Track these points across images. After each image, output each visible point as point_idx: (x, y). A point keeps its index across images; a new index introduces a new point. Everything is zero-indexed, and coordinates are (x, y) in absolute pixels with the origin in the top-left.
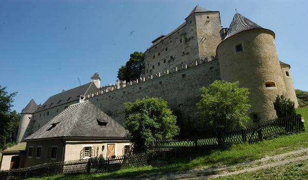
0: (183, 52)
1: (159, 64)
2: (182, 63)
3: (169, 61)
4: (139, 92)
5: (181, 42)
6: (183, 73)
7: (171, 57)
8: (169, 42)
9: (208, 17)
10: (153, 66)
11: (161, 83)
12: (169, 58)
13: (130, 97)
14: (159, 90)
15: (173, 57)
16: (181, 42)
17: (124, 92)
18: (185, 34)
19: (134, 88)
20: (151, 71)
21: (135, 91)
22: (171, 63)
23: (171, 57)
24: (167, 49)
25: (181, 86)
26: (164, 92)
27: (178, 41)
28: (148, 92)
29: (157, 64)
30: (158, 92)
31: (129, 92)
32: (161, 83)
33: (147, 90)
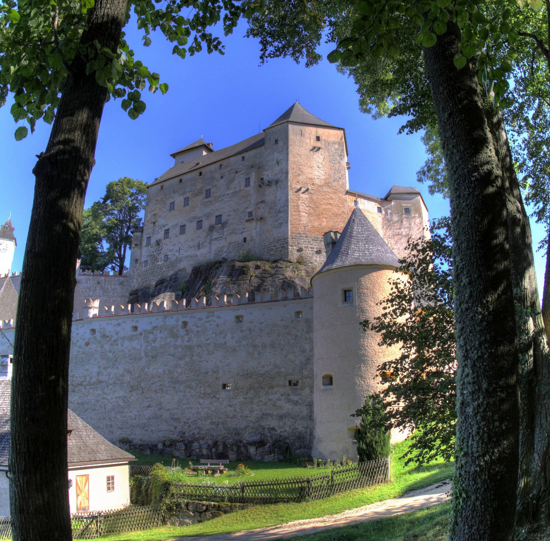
0: (250, 214)
1: (183, 229)
2: (245, 239)
3: (212, 228)
4: (131, 338)
5: (247, 184)
6: (239, 313)
8: (218, 176)
9: (318, 139)
10: (167, 232)
11: (185, 324)
12: (213, 220)
13: (107, 347)
15: (224, 219)
16: (247, 184)
17: (93, 331)
18: (259, 168)
19: (119, 325)
20: (158, 243)
22: (215, 235)
24: (208, 194)
26: (189, 348)
27: (240, 180)
28: (154, 341)
29: (178, 229)
31: (107, 333)
32: (185, 324)
33: (151, 337)
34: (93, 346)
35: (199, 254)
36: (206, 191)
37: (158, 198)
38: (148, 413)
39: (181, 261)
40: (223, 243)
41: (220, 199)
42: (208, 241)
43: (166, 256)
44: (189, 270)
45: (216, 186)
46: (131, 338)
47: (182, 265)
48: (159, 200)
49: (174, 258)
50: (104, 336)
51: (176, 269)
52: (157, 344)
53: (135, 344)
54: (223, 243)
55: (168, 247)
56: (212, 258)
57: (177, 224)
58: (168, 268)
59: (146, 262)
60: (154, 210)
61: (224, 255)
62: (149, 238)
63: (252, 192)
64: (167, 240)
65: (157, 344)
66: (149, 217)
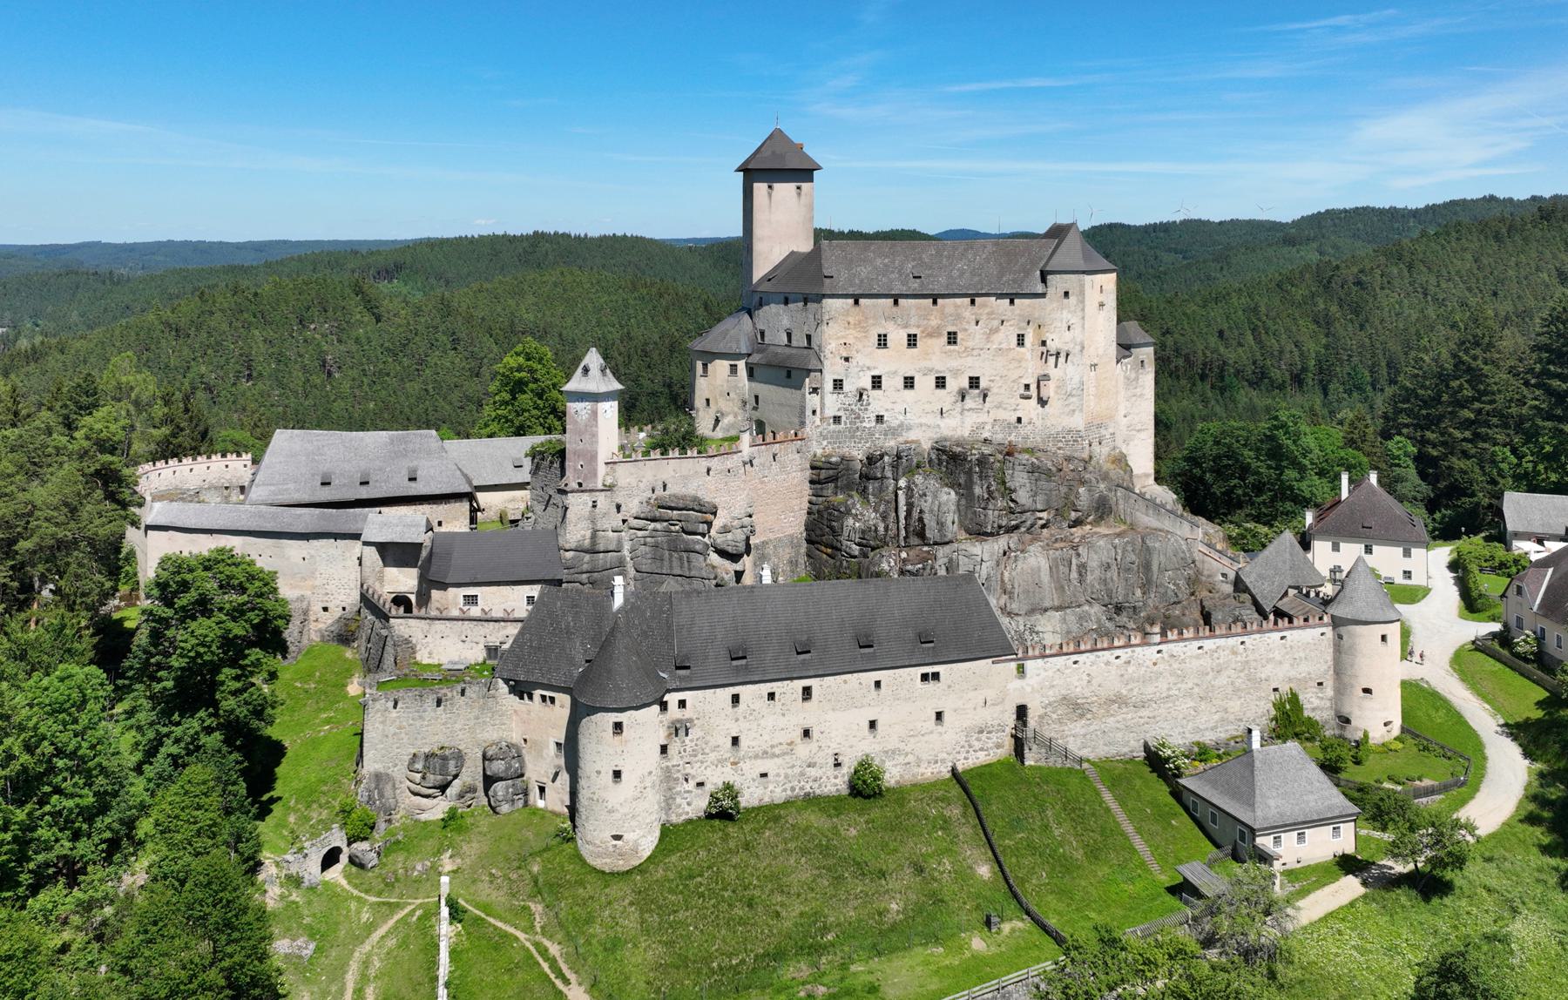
2: (1019, 420)
4: (1198, 657)
5: (1021, 340)
7: (974, 382)
10: (877, 382)
14: (1239, 658)
15: (983, 384)
21: (1189, 654)
22: (969, 403)
23: (974, 382)
24: (952, 338)
25: (1278, 658)
26: (1247, 662)
30: (1236, 662)
33: (1216, 655)
34: (1161, 667)
35: (942, 425)
36: (949, 333)
37: (851, 319)
38: (1216, 717)
39: (909, 428)
40: (983, 417)
41: (975, 353)
42: (959, 410)
43: (880, 419)
44: (926, 446)
45: (966, 330)
46: (1198, 657)
47: (912, 436)
48: (852, 322)
49: (898, 422)
50: (1173, 656)
51: (901, 439)
52: (1221, 661)
53: (1201, 662)
54: (983, 417)
55: (878, 402)
56: (967, 434)
57: (895, 372)
58: (886, 435)
59: (837, 419)
60: (843, 337)
61: (986, 435)
62: (838, 384)
63: (1028, 356)
64: (877, 392)
65: (1221, 661)
66: (833, 345)
